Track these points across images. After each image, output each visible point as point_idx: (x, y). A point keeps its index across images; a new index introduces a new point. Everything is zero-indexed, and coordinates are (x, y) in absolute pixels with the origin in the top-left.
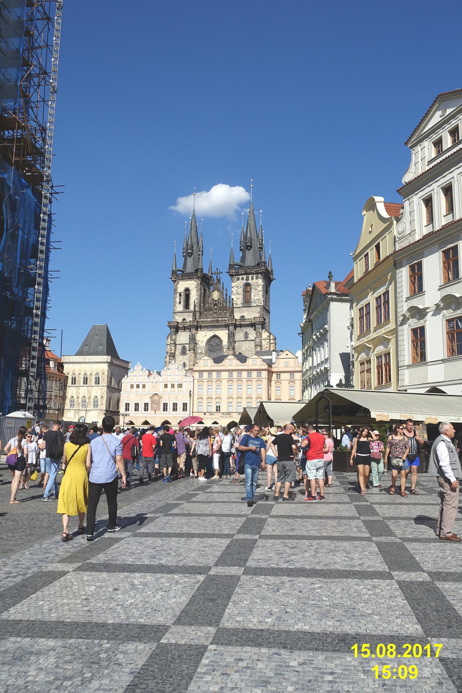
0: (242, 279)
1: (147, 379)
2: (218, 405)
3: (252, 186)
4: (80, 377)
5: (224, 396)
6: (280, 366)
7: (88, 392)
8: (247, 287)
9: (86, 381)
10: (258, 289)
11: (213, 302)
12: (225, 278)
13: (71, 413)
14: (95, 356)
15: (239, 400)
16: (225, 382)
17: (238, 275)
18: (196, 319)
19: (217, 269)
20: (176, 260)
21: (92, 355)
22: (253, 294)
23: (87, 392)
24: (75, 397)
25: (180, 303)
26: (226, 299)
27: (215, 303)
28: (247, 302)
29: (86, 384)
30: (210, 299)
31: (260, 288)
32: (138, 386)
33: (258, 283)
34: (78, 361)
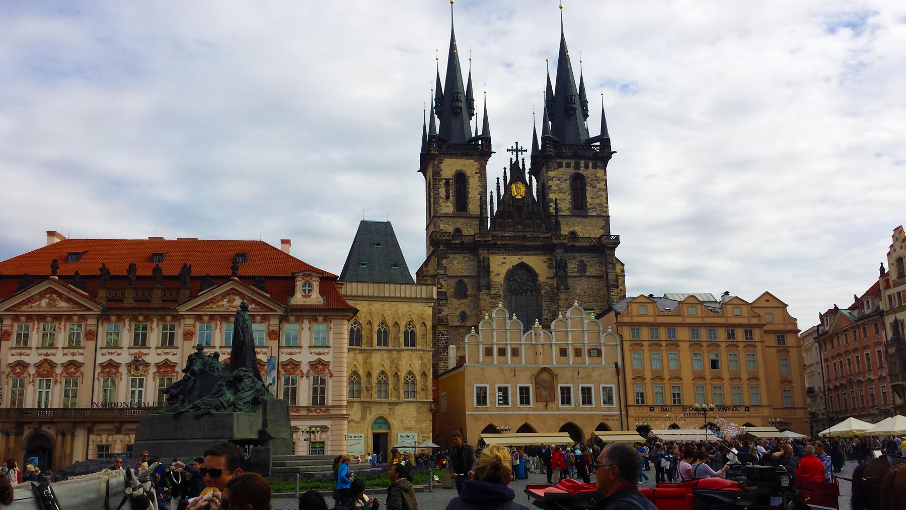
0: (568, 166)
1: (524, 338)
2: (676, 391)
4: (372, 330)
5: (687, 376)
7: (392, 362)
9: (384, 337)
13: (354, 409)
16: (684, 347)
21: (384, 283)
23: (388, 362)
24: (361, 372)
27: (516, 204)
29: (386, 344)
32: (502, 352)
34: (365, 294)
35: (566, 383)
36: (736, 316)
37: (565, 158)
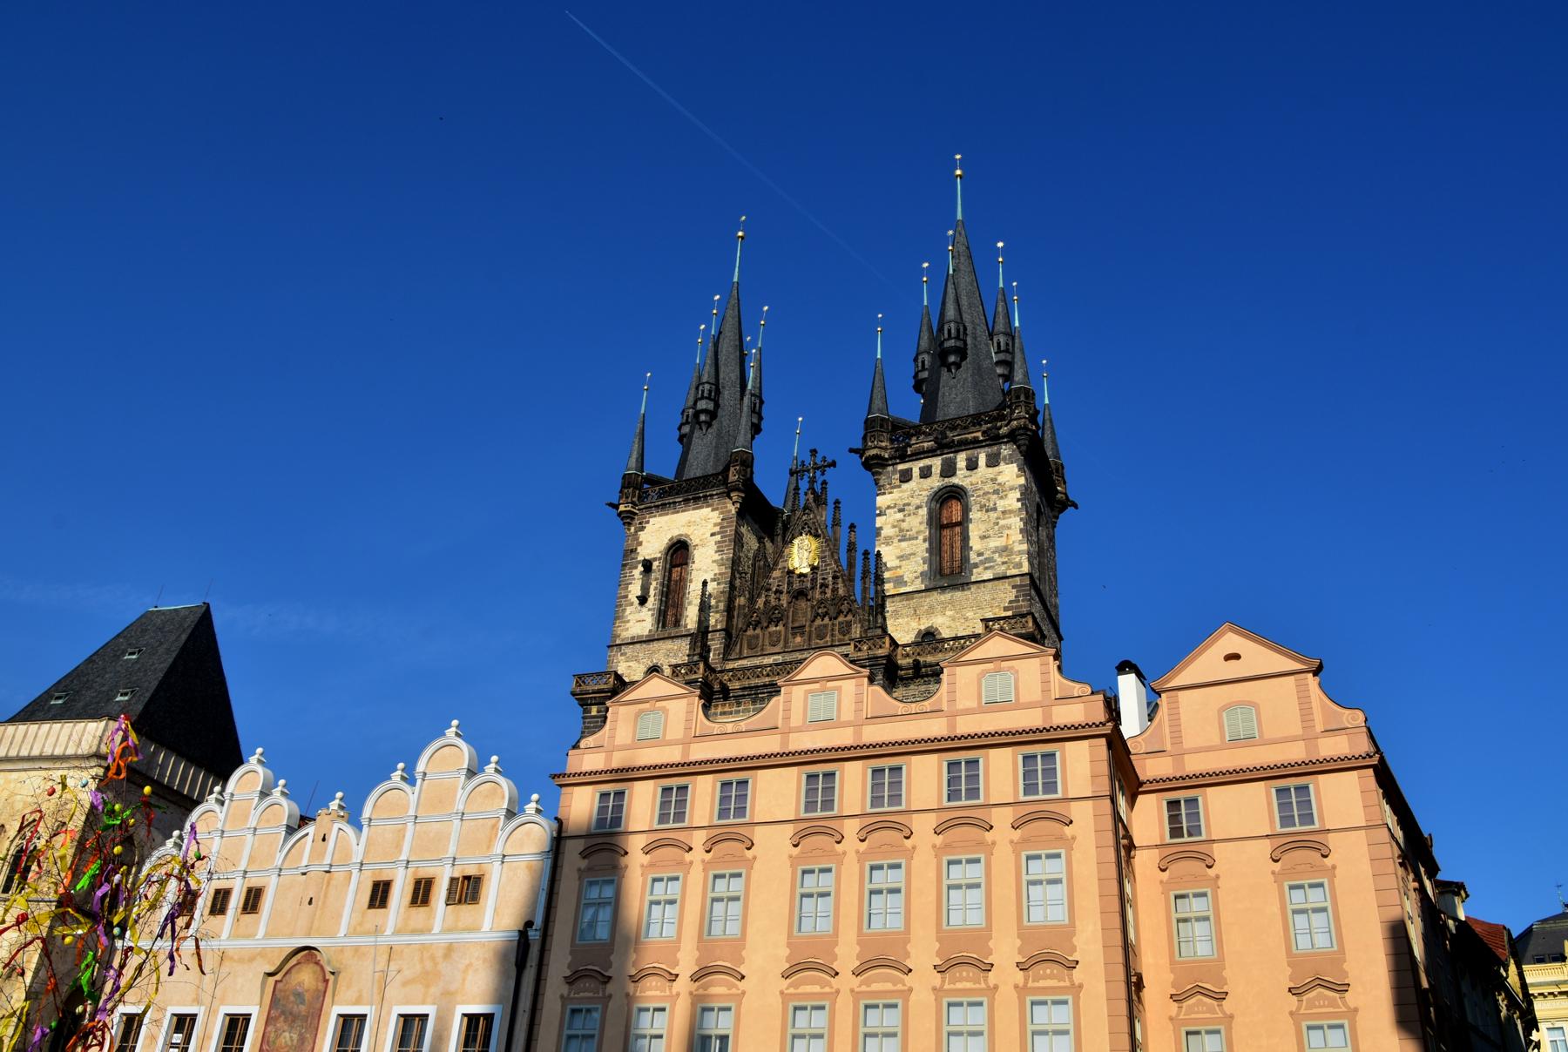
3: (958, 172)
5: (765, 956)
6: (1189, 742)
8: (949, 505)
10: (1001, 505)
11: (790, 584)
12: (844, 479)
14: (46, 727)
15: (881, 982)
17: (904, 458)
18: (704, 657)
19: (814, 452)
20: (642, 439)
22: (974, 532)
25: (643, 600)
26: (851, 565)
27: (796, 586)
28: (949, 571)
30: (776, 574)
31: (1012, 501)
33: (999, 484)
35: (358, 1002)
36: (992, 705)
37: (919, 455)
